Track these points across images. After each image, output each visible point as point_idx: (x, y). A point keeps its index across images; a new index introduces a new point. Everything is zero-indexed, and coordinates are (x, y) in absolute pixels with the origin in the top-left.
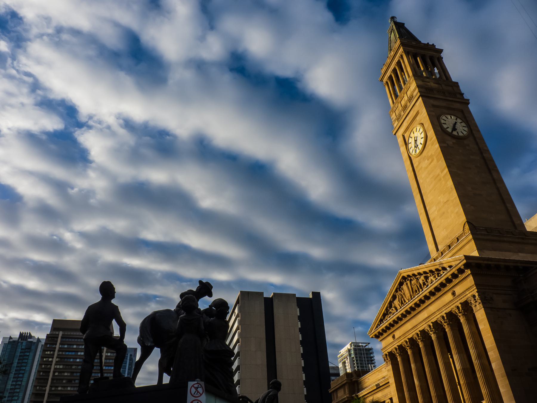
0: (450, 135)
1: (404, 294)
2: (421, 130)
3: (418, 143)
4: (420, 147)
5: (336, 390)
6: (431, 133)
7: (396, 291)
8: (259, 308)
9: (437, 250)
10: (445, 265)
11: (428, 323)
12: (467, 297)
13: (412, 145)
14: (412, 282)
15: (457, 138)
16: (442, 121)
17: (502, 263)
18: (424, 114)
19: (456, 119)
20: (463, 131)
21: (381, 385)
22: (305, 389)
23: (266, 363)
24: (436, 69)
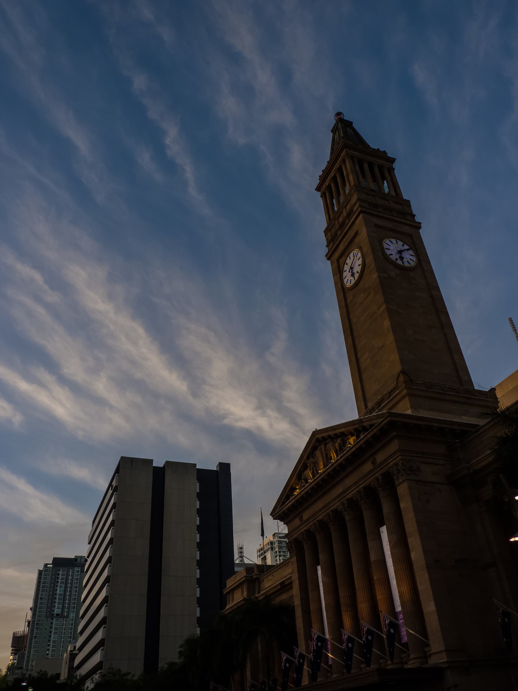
0: (393, 263)
1: (317, 462)
2: (359, 255)
3: (355, 271)
4: (357, 276)
5: (233, 590)
6: (370, 259)
7: (308, 458)
8: (146, 481)
9: (366, 407)
10: (365, 424)
11: (341, 501)
12: (388, 466)
13: (347, 275)
14: (327, 446)
15: (403, 268)
16: (385, 246)
17: (436, 425)
18: (364, 233)
19: (403, 245)
20: (410, 261)
21: (286, 583)
22: (198, 589)
23: (147, 555)
24: (385, 182)
